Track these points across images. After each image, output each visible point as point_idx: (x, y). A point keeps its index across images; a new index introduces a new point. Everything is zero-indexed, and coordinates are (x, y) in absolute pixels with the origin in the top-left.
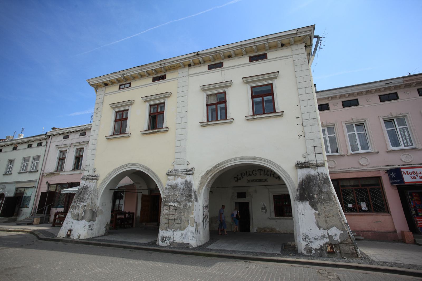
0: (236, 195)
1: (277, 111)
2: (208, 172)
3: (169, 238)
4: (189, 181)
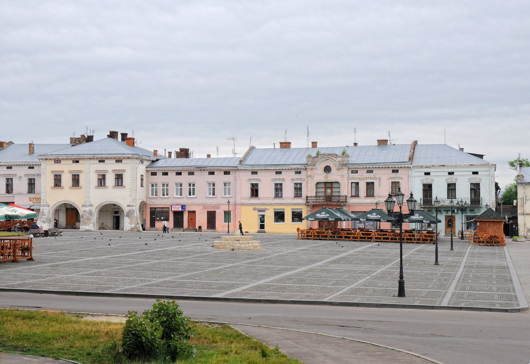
0: (113, 212)
1: (123, 185)
2: (98, 206)
3: (84, 228)
4: (91, 209)
